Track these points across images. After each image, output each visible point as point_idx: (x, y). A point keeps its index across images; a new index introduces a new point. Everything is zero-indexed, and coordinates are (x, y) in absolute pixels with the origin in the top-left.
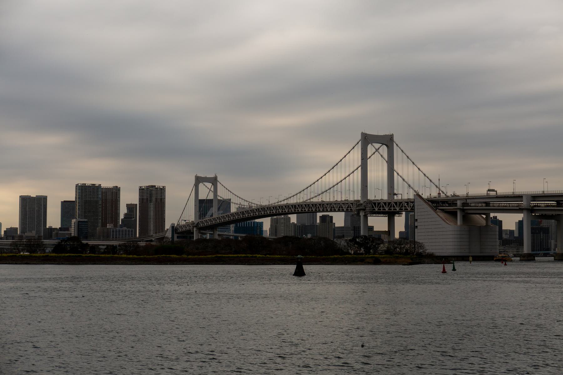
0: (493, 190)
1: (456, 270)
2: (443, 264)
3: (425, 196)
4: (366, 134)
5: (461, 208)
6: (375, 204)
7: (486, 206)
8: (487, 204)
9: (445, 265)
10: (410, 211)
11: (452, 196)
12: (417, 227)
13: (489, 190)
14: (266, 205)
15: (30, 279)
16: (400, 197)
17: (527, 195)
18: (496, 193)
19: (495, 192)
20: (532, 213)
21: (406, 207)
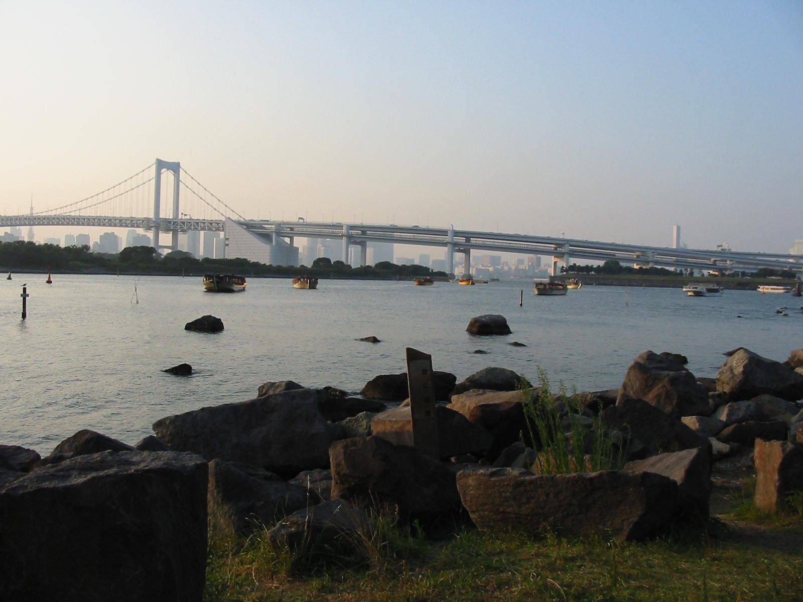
0: (302, 219)
1: (11, 279)
2: (47, 273)
3: (233, 219)
4: (160, 160)
5: (278, 231)
6: (170, 222)
7: (290, 231)
8: (292, 229)
9: (51, 275)
10: (200, 230)
11: (250, 220)
12: (227, 245)
13: (300, 218)
14: (23, 216)
15: (59, 287)
16: (188, 217)
17: (348, 225)
18: (304, 221)
19: (302, 220)
20: (454, 247)
21: (181, 226)
